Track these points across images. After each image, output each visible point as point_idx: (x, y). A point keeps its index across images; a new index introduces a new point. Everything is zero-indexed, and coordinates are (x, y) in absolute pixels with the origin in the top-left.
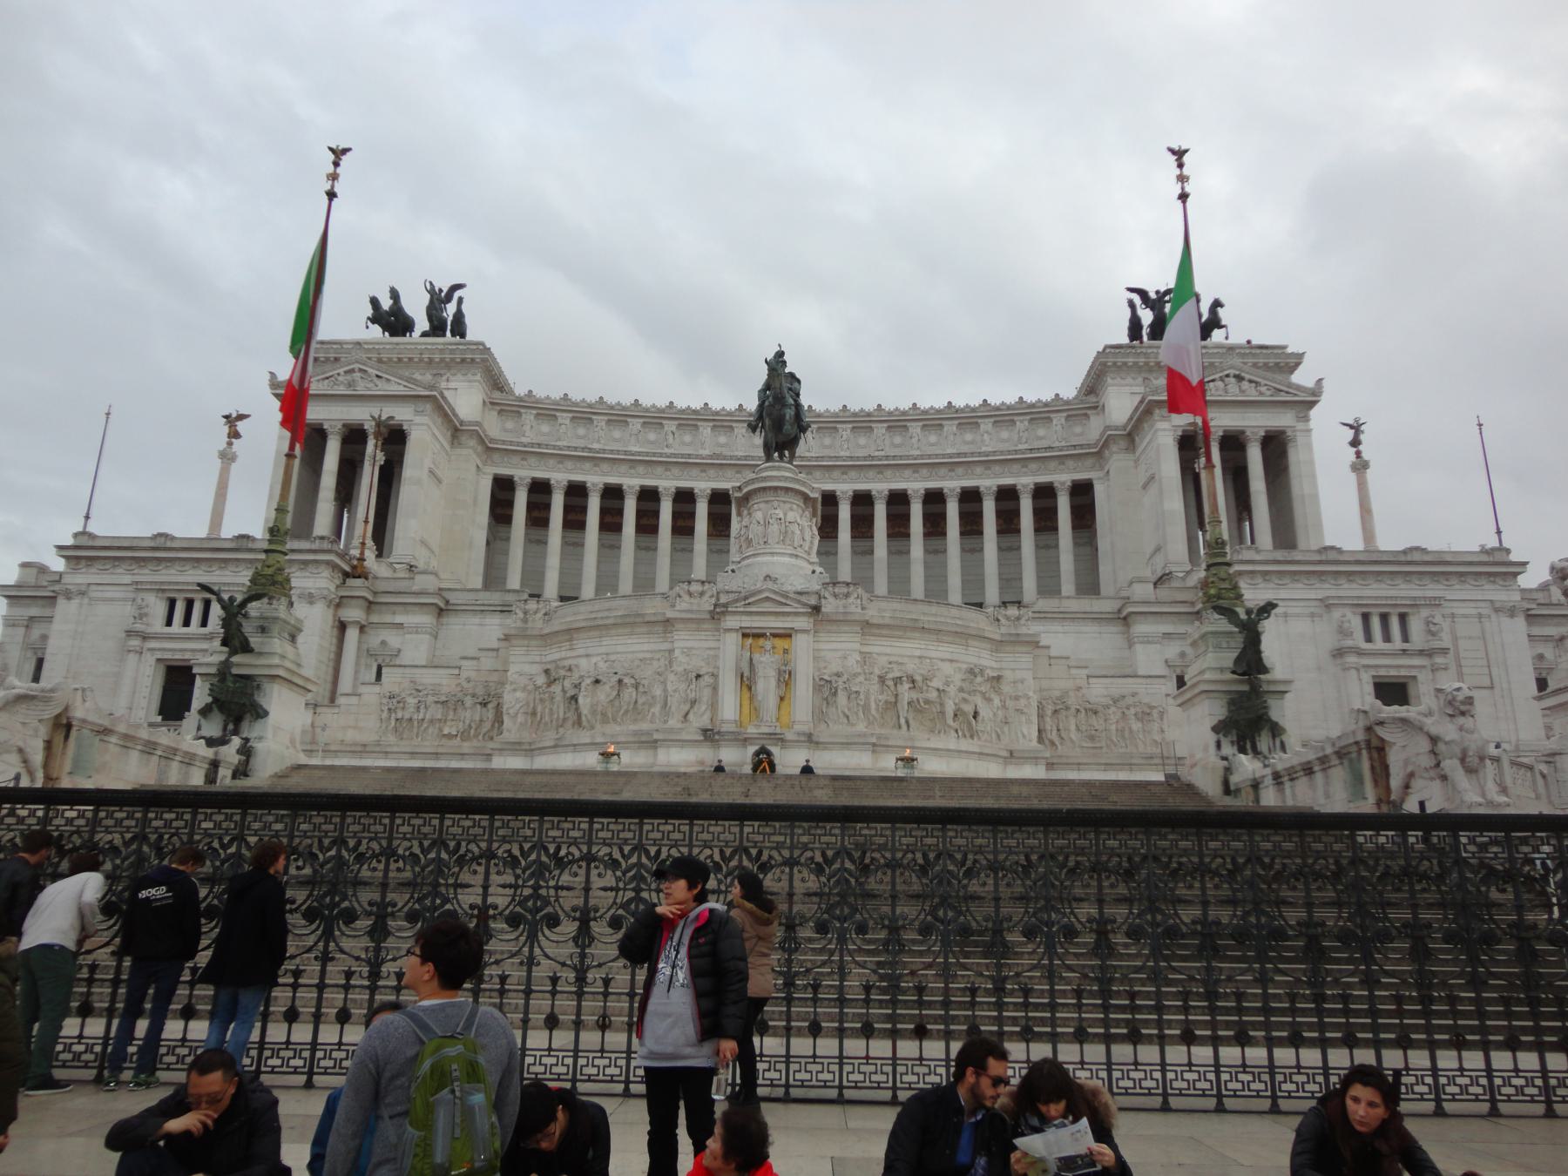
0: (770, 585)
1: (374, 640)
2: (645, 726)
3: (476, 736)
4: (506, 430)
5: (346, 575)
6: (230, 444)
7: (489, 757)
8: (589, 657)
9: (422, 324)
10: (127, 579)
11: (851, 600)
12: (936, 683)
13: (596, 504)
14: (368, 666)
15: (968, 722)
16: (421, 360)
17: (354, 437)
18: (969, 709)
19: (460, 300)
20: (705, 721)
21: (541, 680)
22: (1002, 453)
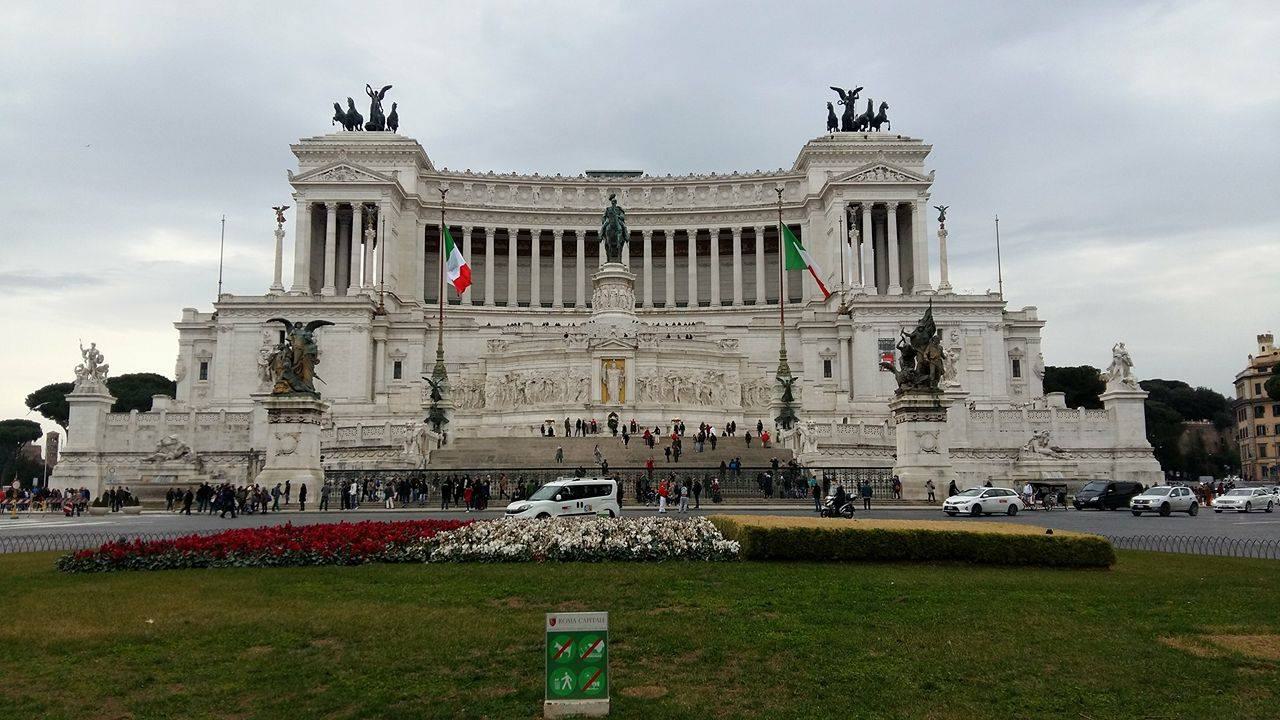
0: (614, 336)
1: (392, 348)
2: (557, 403)
3: (471, 407)
4: (430, 194)
5: (375, 314)
6: (280, 226)
7: (481, 416)
8: (528, 370)
9: (367, 119)
10: (254, 320)
11: (652, 342)
12: (691, 380)
13: (490, 244)
14: (390, 363)
15: (706, 397)
16: (376, 153)
17: (344, 209)
18: (708, 392)
19: (395, 106)
20: (586, 401)
21: (504, 380)
22: (745, 207)
